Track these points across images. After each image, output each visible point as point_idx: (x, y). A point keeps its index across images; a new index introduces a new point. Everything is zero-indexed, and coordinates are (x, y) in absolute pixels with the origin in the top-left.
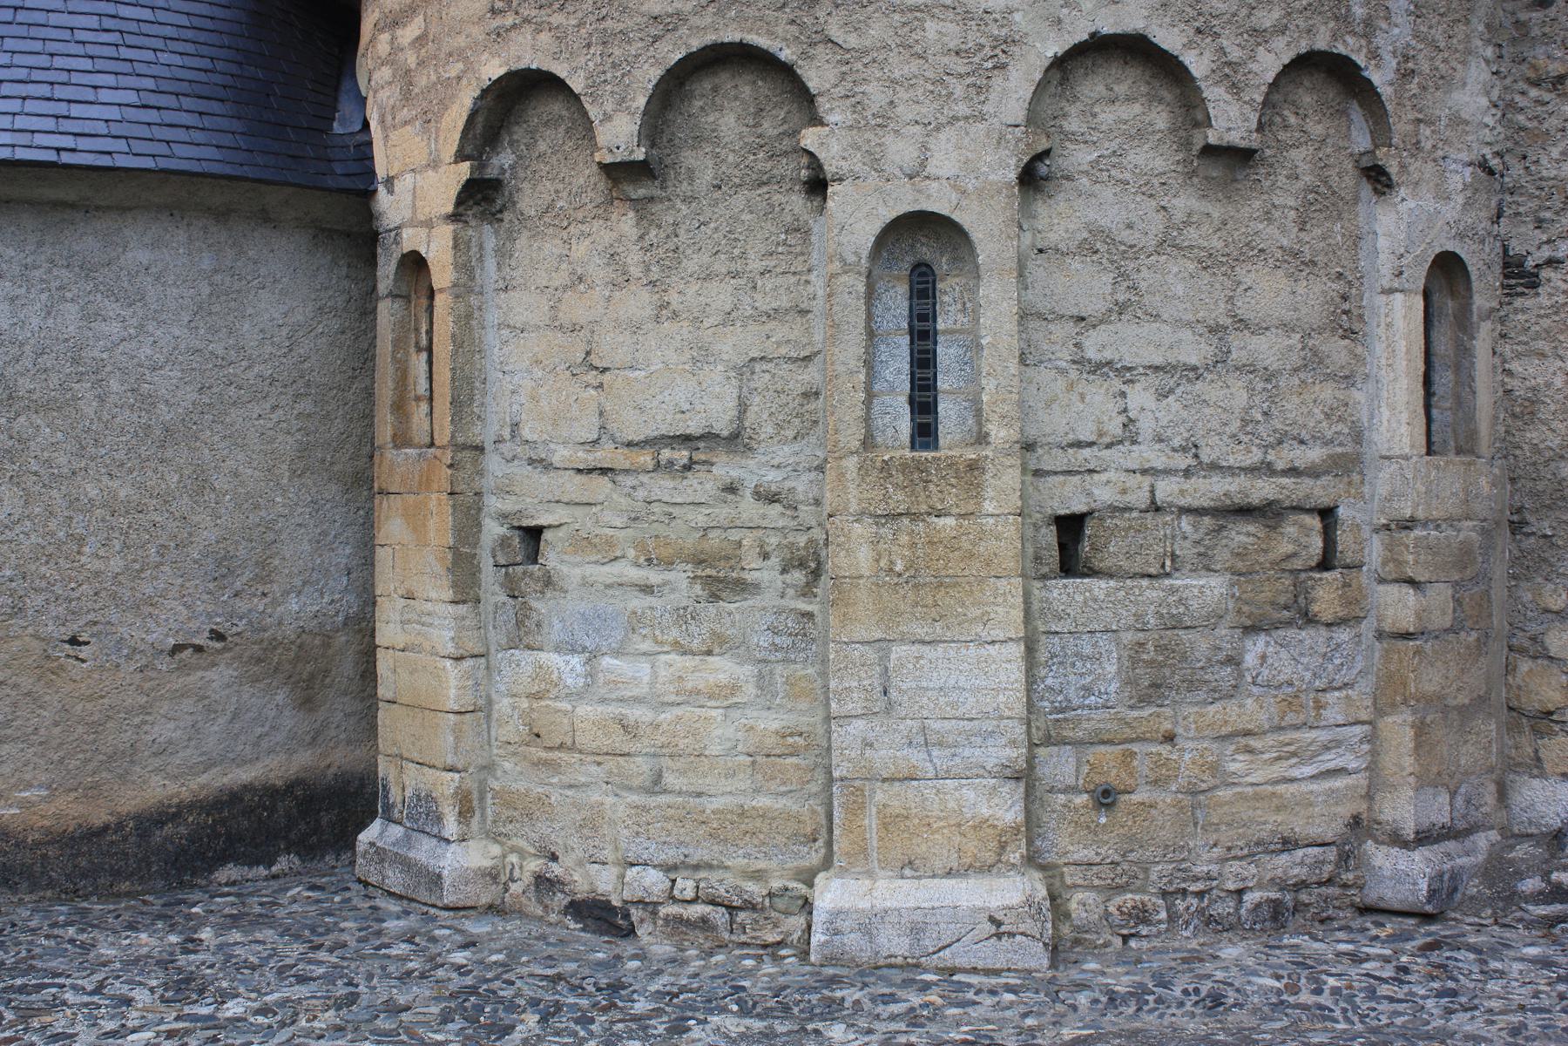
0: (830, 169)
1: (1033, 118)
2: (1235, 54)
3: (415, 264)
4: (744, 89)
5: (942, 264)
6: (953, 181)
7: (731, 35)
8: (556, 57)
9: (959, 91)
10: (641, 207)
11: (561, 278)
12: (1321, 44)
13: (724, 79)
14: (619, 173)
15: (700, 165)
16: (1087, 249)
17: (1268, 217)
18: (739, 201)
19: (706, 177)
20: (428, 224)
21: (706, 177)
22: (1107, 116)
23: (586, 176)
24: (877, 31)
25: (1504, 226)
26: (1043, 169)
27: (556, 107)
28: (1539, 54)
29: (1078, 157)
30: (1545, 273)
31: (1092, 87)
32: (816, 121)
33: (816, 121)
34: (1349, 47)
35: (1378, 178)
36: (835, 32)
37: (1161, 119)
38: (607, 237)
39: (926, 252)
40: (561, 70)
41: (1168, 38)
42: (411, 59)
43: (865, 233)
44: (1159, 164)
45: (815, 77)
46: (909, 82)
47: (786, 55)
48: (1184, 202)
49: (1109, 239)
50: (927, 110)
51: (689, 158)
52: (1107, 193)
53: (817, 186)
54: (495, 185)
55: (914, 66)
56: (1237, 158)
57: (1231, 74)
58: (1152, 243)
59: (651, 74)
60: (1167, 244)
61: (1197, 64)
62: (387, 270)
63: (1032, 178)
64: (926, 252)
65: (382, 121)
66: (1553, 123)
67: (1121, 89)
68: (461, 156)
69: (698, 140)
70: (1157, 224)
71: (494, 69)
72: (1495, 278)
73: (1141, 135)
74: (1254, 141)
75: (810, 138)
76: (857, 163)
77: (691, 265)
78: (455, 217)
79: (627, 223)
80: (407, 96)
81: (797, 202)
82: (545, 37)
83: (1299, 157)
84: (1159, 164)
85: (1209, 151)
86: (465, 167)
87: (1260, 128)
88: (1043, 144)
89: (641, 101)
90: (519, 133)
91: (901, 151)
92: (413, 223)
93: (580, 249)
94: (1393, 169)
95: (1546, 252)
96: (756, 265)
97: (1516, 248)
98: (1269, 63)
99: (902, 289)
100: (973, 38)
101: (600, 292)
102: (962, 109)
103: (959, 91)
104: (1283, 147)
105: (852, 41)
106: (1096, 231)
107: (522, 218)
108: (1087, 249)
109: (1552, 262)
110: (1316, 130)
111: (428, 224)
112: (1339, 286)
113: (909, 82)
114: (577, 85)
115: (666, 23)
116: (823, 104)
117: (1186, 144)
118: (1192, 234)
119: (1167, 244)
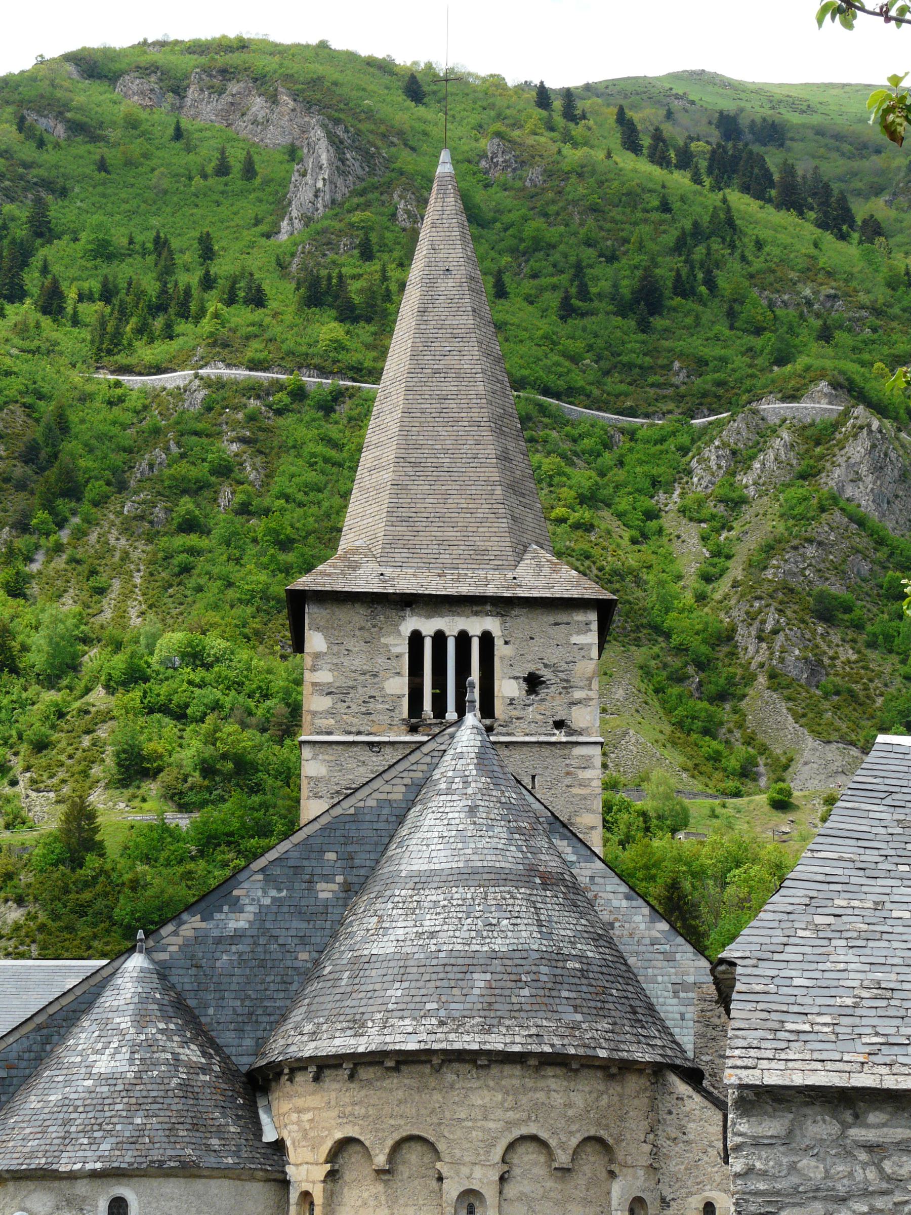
0: (444, 1175)
1: (504, 1161)
2: (564, 1139)
3: (306, 1196)
4: (418, 1148)
5: (477, 1204)
6: (480, 1180)
7: (416, 1132)
8: (361, 1134)
9: (482, 1152)
10: (386, 1182)
11: (359, 1203)
12: (592, 1133)
13: (412, 1144)
14: (379, 1172)
15: (404, 1171)
16: (519, 1199)
17: (576, 1188)
18: (416, 1182)
19: (406, 1175)
20: (313, 1182)
21: (406, 1175)
22: (526, 1158)
23: (367, 1171)
24: (459, 1133)
25: (660, 1186)
26: (506, 1176)
27: (358, 1148)
28: (669, 1129)
29: (517, 1171)
30: (672, 1203)
31: (521, 1149)
32: (439, 1159)
33: (439, 1159)
34: (602, 1133)
35: (612, 1174)
36: (446, 1134)
37: (542, 1159)
38: (375, 1191)
39: (472, 1200)
40: (362, 1138)
41: (543, 1135)
42: (308, 1127)
43: (455, 1194)
44: (542, 1172)
45: (441, 1146)
46: (467, 1150)
47: (432, 1139)
48: (549, 1184)
49: (526, 1196)
50: (473, 1159)
51: (401, 1168)
52: (526, 1182)
53: (440, 1179)
54: (337, 1171)
55: (469, 1145)
56: (565, 1171)
57: (562, 1145)
58: (539, 1197)
59: (390, 1143)
60: (545, 1197)
61: (553, 1143)
62: (294, 1196)
63: (502, 1179)
64: (472, 1200)
65: (293, 1143)
66: (673, 1153)
67: (530, 1150)
68: (327, 1162)
69: (404, 1163)
70: (541, 1191)
71: (339, 1135)
72: (658, 1203)
73: (536, 1164)
74: (570, 1166)
75: (438, 1165)
76: (452, 1173)
77: (401, 1201)
78: (324, 1181)
79: (380, 1187)
80: (305, 1137)
81: (434, 1184)
82: (357, 1127)
83: (587, 1169)
84: (542, 1172)
85: (556, 1169)
86: (329, 1165)
87: (573, 1160)
88: (506, 1169)
89: (387, 1151)
90: (345, 1155)
91: (465, 1170)
92: (307, 1181)
93: (366, 1195)
94: (617, 1171)
95: (672, 1196)
96: (421, 1202)
97: (664, 1194)
98: (574, 1141)
99: (465, 1211)
100: (486, 1137)
101: (371, 1209)
102: (483, 1158)
103: (482, 1152)
104: (581, 1165)
105: (451, 1137)
106: (522, 1193)
107: (345, 1182)
108: (519, 1199)
109: (673, 1199)
110: (592, 1159)
111: (313, 1182)
112: (600, 1209)
113: (467, 1150)
114: (367, 1143)
115: (397, 1128)
116: (442, 1155)
117: (550, 1166)
118: (552, 1194)
119: (545, 1197)
